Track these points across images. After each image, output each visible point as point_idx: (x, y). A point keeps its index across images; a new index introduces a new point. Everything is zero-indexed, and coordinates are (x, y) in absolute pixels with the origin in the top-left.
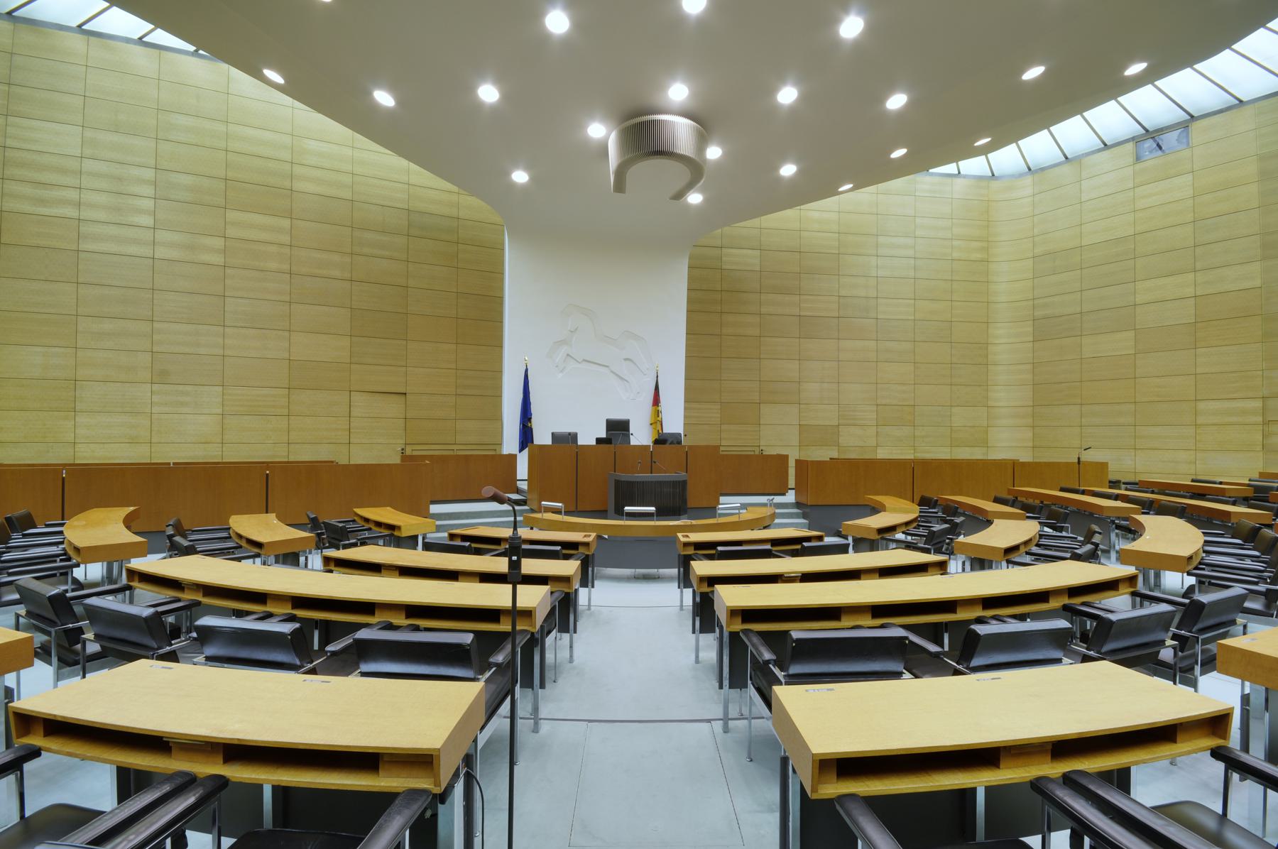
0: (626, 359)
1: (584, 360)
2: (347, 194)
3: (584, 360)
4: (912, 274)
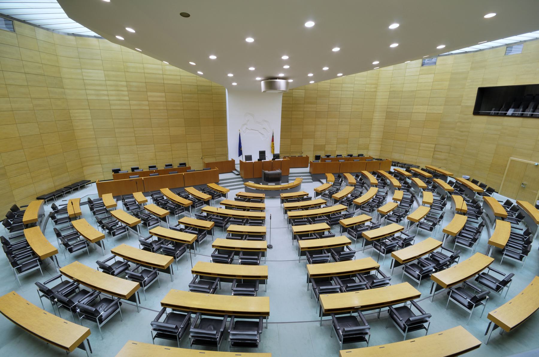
0: (263, 128)
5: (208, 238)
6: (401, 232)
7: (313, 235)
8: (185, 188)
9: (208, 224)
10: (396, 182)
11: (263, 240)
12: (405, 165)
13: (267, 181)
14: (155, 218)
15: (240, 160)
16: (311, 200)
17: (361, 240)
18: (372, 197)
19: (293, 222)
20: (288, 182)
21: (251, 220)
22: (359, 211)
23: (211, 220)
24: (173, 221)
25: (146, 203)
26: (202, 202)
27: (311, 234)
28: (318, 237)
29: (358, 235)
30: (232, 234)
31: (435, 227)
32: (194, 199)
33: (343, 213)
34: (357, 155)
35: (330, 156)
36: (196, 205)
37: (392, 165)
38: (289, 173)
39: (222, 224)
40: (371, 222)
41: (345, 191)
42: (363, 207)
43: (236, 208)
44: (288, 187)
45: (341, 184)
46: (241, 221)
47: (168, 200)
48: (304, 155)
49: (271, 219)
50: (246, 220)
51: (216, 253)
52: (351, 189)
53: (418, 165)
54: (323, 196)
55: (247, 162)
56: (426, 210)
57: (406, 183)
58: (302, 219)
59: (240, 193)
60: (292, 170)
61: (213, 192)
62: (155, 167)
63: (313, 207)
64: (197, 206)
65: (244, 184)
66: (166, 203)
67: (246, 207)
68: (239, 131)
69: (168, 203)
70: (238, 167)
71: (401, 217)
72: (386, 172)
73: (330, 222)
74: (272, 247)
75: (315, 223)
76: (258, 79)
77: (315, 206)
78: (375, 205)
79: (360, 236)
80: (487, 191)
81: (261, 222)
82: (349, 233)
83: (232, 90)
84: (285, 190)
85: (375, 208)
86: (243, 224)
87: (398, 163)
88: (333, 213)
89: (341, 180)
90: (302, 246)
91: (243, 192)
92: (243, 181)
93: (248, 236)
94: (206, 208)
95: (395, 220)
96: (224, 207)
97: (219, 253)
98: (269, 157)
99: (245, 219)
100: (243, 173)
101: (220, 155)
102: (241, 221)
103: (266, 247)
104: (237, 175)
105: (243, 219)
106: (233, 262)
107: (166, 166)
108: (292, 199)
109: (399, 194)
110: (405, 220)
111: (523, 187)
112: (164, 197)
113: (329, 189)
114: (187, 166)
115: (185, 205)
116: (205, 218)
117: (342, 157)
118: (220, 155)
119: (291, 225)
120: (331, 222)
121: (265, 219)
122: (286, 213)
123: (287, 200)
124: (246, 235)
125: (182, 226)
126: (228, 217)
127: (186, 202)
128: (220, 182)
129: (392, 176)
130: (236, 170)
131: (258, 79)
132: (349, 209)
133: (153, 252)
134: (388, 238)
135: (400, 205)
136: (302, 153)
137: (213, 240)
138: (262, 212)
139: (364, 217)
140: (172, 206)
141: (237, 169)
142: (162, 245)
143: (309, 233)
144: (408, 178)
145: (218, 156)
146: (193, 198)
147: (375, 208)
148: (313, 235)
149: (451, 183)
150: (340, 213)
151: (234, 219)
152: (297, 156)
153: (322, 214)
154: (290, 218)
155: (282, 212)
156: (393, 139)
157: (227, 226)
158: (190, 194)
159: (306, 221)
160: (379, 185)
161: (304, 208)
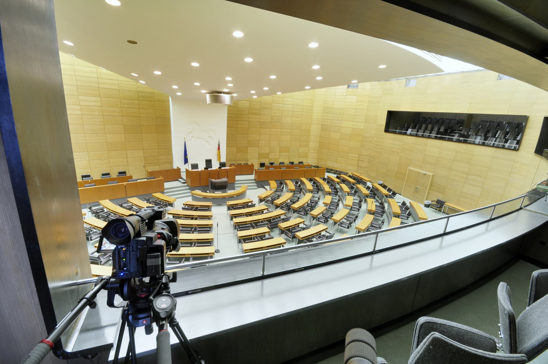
0: (209, 137)
2: (117, 88)
4: (292, 110)
6: (325, 231)
7: (255, 238)
8: (129, 199)
10: (327, 188)
12: (337, 171)
13: (213, 189)
14: (97, 232)
15: (186, 169)
16: (255, 207)
17: (295, 240)
18: (307, 203)
19: (238, 228)
20: (234, 189)
21: (200, 228)
22: (296, 215)
25: (85, 216)
27: (254, 237)
28: (260, 239)
29: (292, 236)
31: (351, 225)
32: (138, 209)
33: (282, 217)
34: (297, 163)
35: (274, 163)
37: (327, 172)
38: (235, 181)
40: (304, 224)
41: (286, 197)
42: (299, 211)
43: (183, 218)
44: (235, 195)
45: (282, 190)
46: (190, 229)
47: (110, 212)
48: (250, 163)
49: (218, 226)
50: (194, 228)
52: (291, 194)
53: (347, 172)
54: (266, 202)
55: (194, 170)
56: (347, 211)
57: (335, 188)
58: (247, 224)
59: (187, 202)
60: (238, 178)
61: (159, 202)
62: (89, 176)
65: (191, 193)
66: (108, 216)
67: (193, 216)
68: (185, 139)
69: (110, 215)
70: (184, 175)
73: (270, 226)
74: (219, 252)
75: (257, 228)
77: (258, 212)
78: (309, 209)
79: (294, 237)
80: (392, 194)
81: (209, 229)
82: (286, 234)
83: (175, 98)
84: (231, 198)
85: (309, 212)
86: (192, 232)
87: (332, 170)
89: (282, 186)
91: (189, 201)
92: (190, 189)
93: (196, 243)
95: (324, 222)
97: (169, 260)
98: (215, 166)
99: (193, 227)
100: (189, 181)
102: (190, 229)
103: (214, 252)
104: (184, 183)
105: (192, 228)
107: (103, 175)
108: (238, 206)
109: (328, 199)
110: (331, 221)
111: (417, 190)
112: (104, 209)
113: (272, 195)
114: (128, 175)
119: (236, 230)
120: (272, 226)
121: (212, 227)
122: (232, 219)
123: (233, 207)
124: (195, 242)
128: (165, 191)
129: (325, 182)
130: (181, 178)
132: (289, 213)
133: (101, 265)
134: (315, 237)
135: (329, 208)
136: (248, 160)
138: (209, 220)
139: (299, 220)
141: (182, 177)
143: (253, 236)
144: (337, 184)
145: (161, 164)
146: (137, 209)
147: (309, 212)
148: (255, 238)
149: (368, 188)
150: (280, 217)
151: (183, 228)
153: (264, 219)
154: (235, 224)
155: (229, 218)
158: (133, 205)
159: (250, 226)
160: (314, 191)
161: (248, 214)
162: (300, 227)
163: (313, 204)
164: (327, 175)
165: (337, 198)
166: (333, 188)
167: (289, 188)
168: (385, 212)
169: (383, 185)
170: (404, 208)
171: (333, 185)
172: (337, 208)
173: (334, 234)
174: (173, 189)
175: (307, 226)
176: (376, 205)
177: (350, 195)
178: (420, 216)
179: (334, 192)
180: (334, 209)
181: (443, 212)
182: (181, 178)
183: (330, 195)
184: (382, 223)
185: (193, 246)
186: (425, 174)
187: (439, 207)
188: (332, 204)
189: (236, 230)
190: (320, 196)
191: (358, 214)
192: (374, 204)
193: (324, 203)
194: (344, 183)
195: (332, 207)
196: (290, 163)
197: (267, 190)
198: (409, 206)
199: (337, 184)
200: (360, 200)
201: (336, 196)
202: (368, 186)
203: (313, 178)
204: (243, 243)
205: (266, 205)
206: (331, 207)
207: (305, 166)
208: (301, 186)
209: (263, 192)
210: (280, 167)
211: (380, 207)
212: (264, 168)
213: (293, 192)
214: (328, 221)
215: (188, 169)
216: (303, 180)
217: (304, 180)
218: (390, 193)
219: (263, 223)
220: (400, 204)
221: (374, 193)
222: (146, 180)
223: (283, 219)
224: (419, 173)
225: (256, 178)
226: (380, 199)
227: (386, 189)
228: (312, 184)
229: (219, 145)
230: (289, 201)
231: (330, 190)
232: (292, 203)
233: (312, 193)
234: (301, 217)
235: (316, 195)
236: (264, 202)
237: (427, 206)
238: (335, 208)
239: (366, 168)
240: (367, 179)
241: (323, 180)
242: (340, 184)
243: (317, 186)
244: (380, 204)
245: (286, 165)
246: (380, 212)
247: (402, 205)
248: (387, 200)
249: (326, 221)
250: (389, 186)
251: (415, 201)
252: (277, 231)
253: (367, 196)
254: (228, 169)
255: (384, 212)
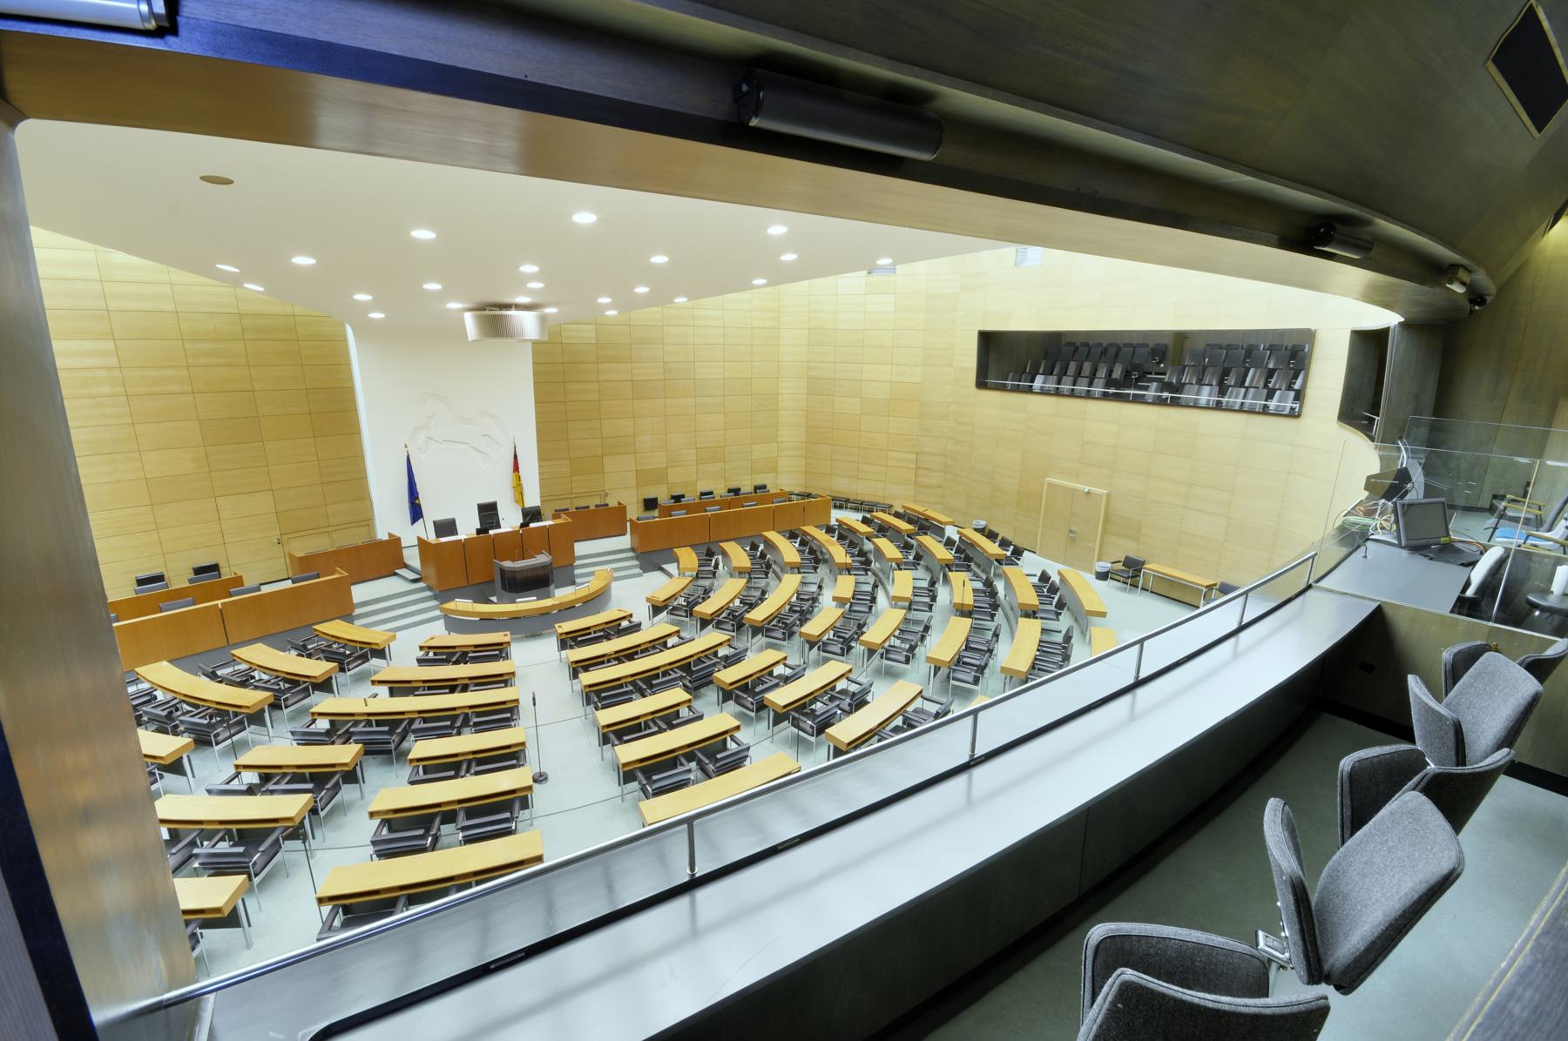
1: (444, 441)
3: (444, 441)
4: (722, 341)
5: (348, 792)
6: (847, 678)
7: (651, 724)
8: (235, 652)
9: (343, 754)
10: (839, 554)
11: (519, 766)
12: (861, 504)
16: (639, 630)
17: (764, 713)
18: (789, 602)
19: (596, 700)
20: (573, 583)
21: (479, 715)
22: (760, 640)
23: (350, 739)
24: (213, 767)
26: (306, 689)
27: (645, 722)
28: (664, 726)
30: (424, 767)
31: (915, 652)
32: (273, 681)
33: (722, 652)
36: (285, 700)
37: (835, 507)
38: (574, 558)
39: (389, 743)
40: (786, 665)
41: (727, 591)
42: (769, 630)
43: (424, 690)
44: (577, 600)
45: (714, 573)
46: (449, 723)
47: (176, 701)
48: (613, 503)
49: (534, 704)
50: (461, 718)
51: (385, 831)
52: (739, 584)
53: (888, 502)
54: (671, 614)
55: (443, 540)
56: (898, 615)
57: (862, 553)
58: (621, 686)
59: (432, 638)
60: (581, 548)
61: (342, 650)
63: (646, 650)
64: (289, 702)
65: (442, 610)
66: (171, 712)
67: (455, 680)
68: (406, 447)
69: (177, 710)
70: (412, 557)
71: (850, 642)
72: (816, 527)
73: (690, 682)
74: (546, 779)
75: (654, 693)
76: (454, 305)
77: (652, 644)
79: (761, 706)
81: (508, 715)
82: (738, 701)
84: (568, 610)
86: (455, 732)
87: (848, 501)
88: (699, 659)
89: (713, 562)
90: (623, 760)
91: (438, 633)
93: (473, 764)
94: (325, 703)
95: (839, 651)
96: (384, 690)
97: (391, 830)
98: (510, 520)
99: (457, 716)
100: (432, 572)
101: (347, 526)
102: (449, 723)
103: (530, 782)
105: (454, 718)
106: (438, 845)
107: (141, 582)
108: (590, 634)
109: (845, 586)
110: (858, 649)
111: (1072, 537)
112: (155, 693)
113: (685, 591)
114: (226, 573)
115: (248, 707)
116: (328, 737)
117: (714, 498)
118: (347, 526)
119: (592, 706)
120: (694, 682)
122: (575, 675)
123: (574, 639)
124: (470, 762)
125: (251, 777)
126: (403, 720)
127: (249, 698)
130: (406, 566)
131: (454, 305)
132: (740, 637)
135: (850, 611)
137: (362, 798)
138: (506, 686)
139: (771, 656)
140: (195, 720)
142: (196, 851)
143: (642, 720)
144: (867, 538)
145: (338, 528)
147: (795, 628)
148: (651, 724)
149: (949, 543)
150: (715, 654)
151: (424, 723)
152: (592, 508)
154: (587, 690)
155: (566, 673)
156: (828, 444)
157: (405, 745)
158: (253, 667)
162: (775, 674)
163: (806, 606)
164: (836, 516)
165: (871, 579)
166: (856, 551)
167: (734, 565)
168: (999, 606)
169: (987, 531)
170: (1045, 590)
171: (854, 543)
172: (874, 608)
173: (871, 685)
174: (387, 600)
175: (795, 671)
176: (973, 590)
177: (903, 567)
178: (1088, 607)
179: (862, 563)
180: (866, 612)
181: (1142, 589)
182: (406, 566)
183: (851, 575)
184: (995, 638)
185: (463, 774)
186: (1088, 492)
187: (1132, 577)
188: (858, 597)
189: (592, 706)
190: (822, 580)
191: (931, 617)
192: (970, 585)
193: (835, 599)
194: (885, 536)
195: (858, 609)
196: (730, 491)
197: (670, 575)
198: (1057, 581)
199: (866, 541)
200: (932, 578)
201: (867, 574)
202: (949, 539)
203: (797, 529)
204: (617, 742)
205: (673, 623)
206: (855, 608)
207: (772, 498)
208: (768, 556)
209: (660, 584)
210: (701, 507)
211: (984, 592)
212: (656, 513)
213: (747, 575)
214: (850, 648)
215: (425, 538)
216: (769, 537)
217: (772, 535)
218: (1008, 550)
219: (668, 678)
220: (1035, 580)
221: (965, 556)
222: (288, 584)
223: (726, 658)
224: (1074, 491)
225: (636, 545)
226: (983, 571)
227: (995, 542)
228: (797, 545)
229: (516, 457)
230: (737, 602)
231: (849, 560)
232: (746, 607)
233: (799, 573)
234: (776, 644)
235: (812, 578)
236: (664, 614)
237: (1103, 576)
238: (866, 609)
239: (940, 486)
240: (943, 518)
241: (826, 532)
242: (874, 540)
243: (812, 552)
244: (985, 585)
245: (717, 498)
246: (987, 606)
247: (1040, 580)
248: (1000, 571)
249: (846, 649)
250: (1004, 533)
251: (1072, 565)
252: (711, 695)
253: (949, 567)
254: (550, 526)
255: (995, 606)
